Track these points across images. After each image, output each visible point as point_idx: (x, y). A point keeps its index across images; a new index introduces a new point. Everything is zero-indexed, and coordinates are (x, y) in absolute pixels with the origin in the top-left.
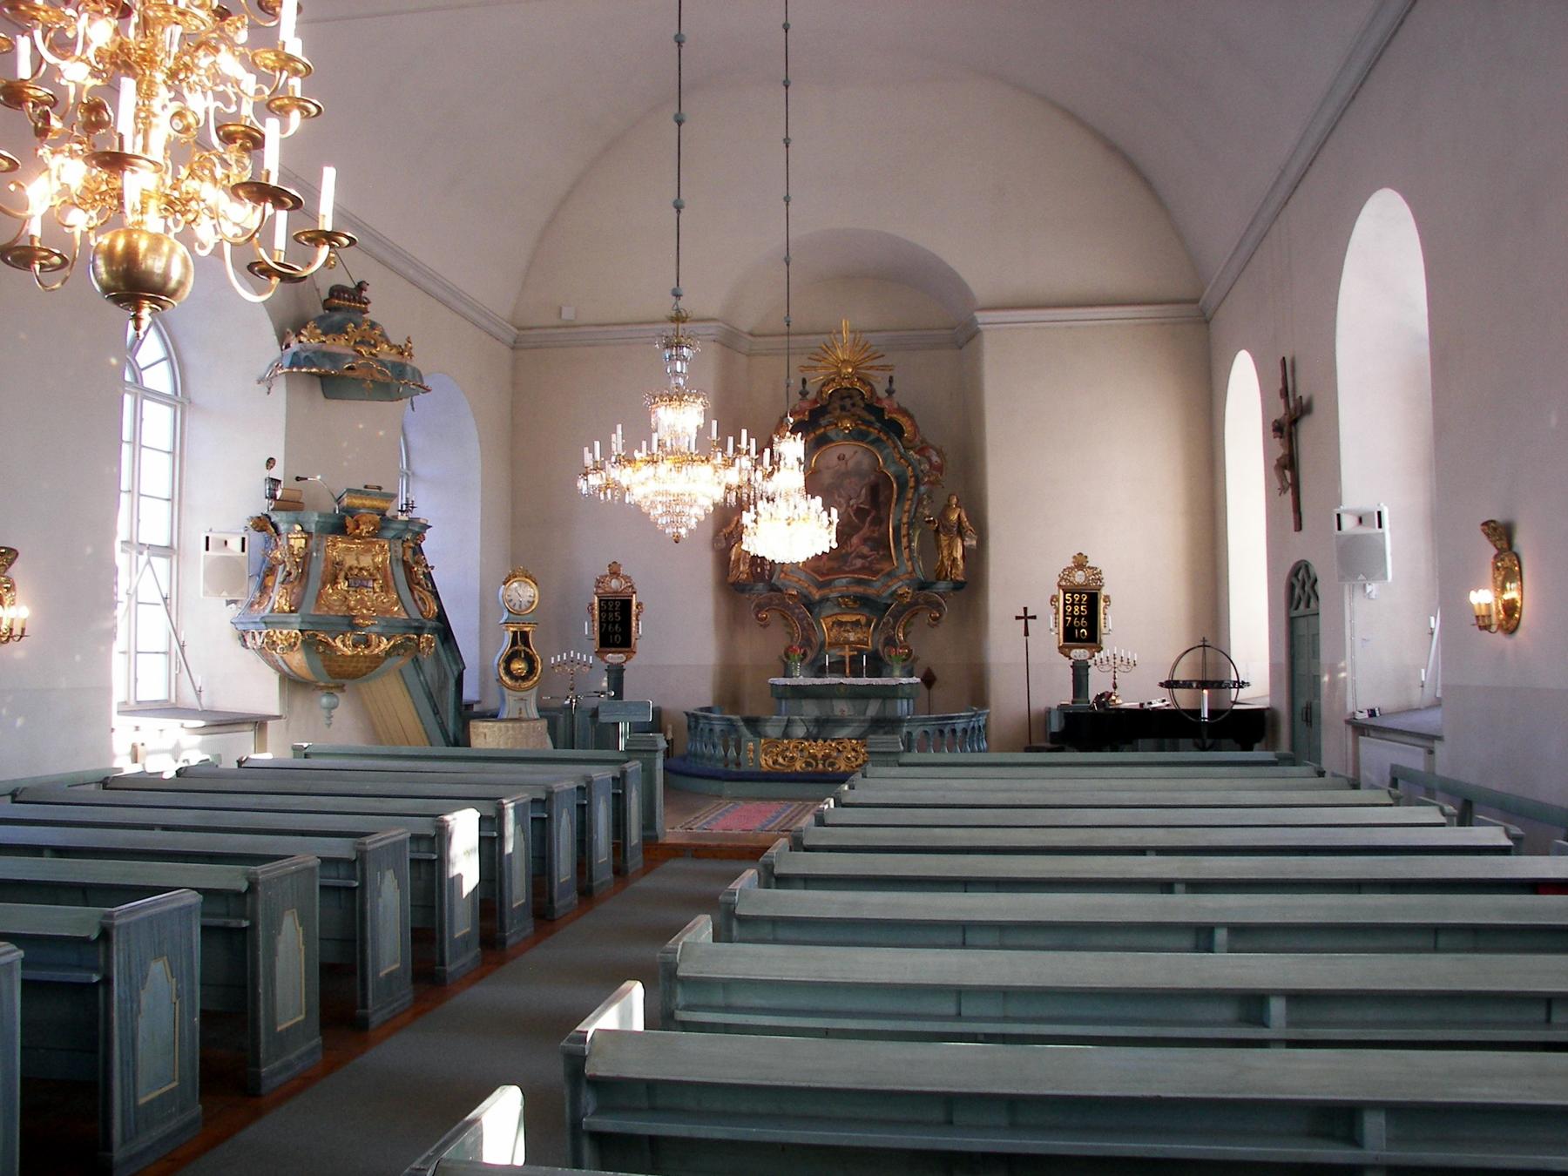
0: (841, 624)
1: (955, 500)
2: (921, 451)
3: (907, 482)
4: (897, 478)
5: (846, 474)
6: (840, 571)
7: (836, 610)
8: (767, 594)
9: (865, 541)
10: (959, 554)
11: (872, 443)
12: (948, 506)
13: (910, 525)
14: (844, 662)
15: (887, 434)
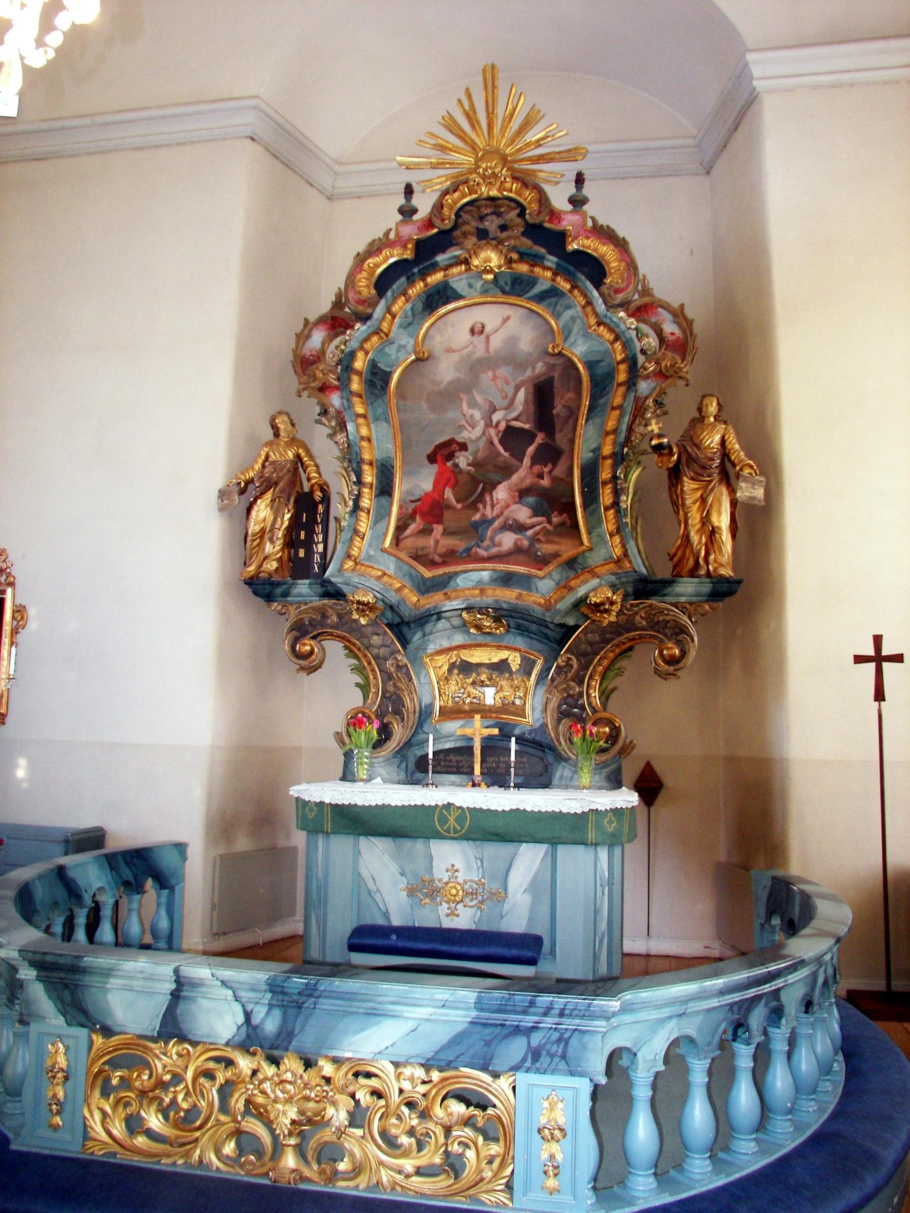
0: (466, 668)
1: (713, 408)
2: (641, 311)
3: (610, 375)
4: (590, 365)
5: (487, 363)
6: (469, 557)
7: (459, 639)
8: (317, 602)
9: (522, 494)
11: (541, 298)
12: (700, 419)
13: (619, 459)
14: (469, 750)
15: (570, 277)
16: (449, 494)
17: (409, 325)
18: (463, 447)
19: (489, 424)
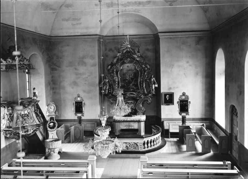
5: (129, 70)
7: (127, 100)
10: (154, 88)
16: (125, 85)
17: (121, 66)
18: (127, 80)
19: (129, 77)
